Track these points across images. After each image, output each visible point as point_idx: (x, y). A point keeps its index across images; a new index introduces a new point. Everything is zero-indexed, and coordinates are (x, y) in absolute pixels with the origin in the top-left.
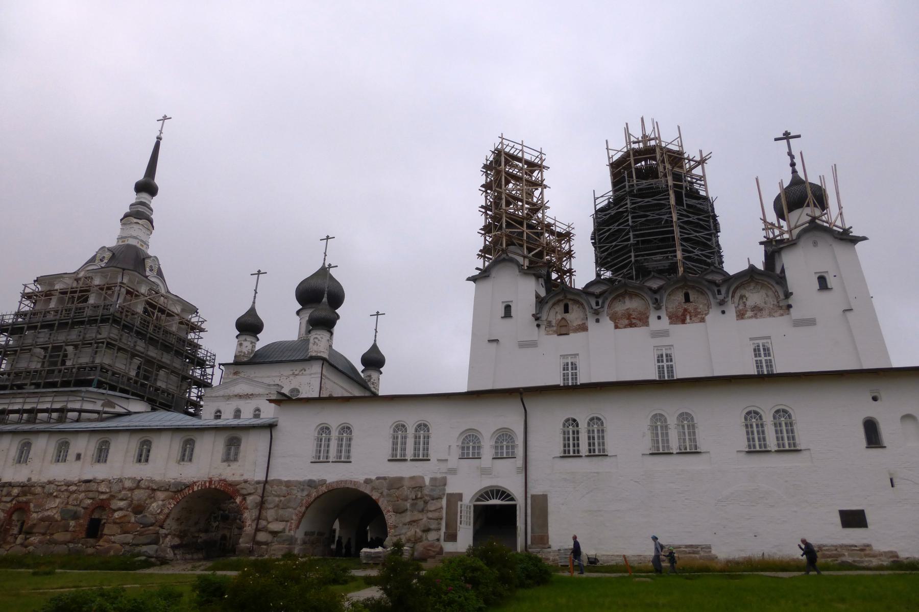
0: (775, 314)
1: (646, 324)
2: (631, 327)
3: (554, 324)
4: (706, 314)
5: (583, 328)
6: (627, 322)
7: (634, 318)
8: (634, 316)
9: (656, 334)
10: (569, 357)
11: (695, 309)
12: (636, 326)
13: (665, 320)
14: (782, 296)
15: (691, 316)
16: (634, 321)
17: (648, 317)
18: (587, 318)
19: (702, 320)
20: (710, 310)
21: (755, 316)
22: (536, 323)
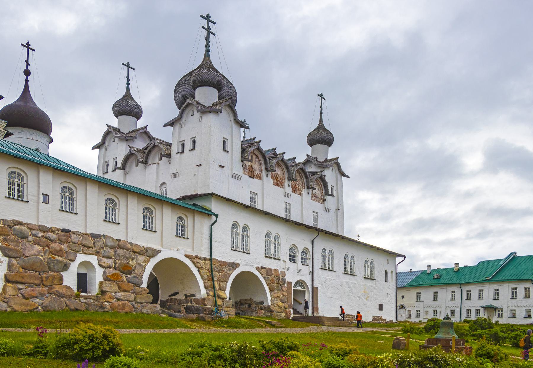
0: (320, 202)
1: (283, 187)
2: (277, 186)
3: (247, 168)
4: (302, 191)
5: (260, 178)
6: (276, 181)
7: (278, 181)
8: (278, 179)
9: (287, 195)
10: (253, 194)
11: (299, 186)
12: (279, 186)
13: (290, 188)
14: (324, 194)
15: (297, 190)
16: (279, 183)
17: (283, 183)
18: (262, 171)
19: (300, 194)
20: (303, 190)
21: (314, 200)
22: (241, 163)
